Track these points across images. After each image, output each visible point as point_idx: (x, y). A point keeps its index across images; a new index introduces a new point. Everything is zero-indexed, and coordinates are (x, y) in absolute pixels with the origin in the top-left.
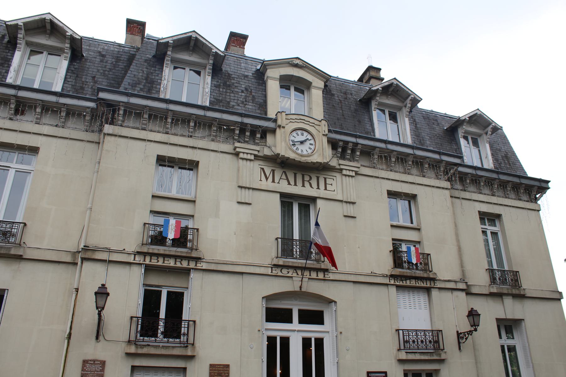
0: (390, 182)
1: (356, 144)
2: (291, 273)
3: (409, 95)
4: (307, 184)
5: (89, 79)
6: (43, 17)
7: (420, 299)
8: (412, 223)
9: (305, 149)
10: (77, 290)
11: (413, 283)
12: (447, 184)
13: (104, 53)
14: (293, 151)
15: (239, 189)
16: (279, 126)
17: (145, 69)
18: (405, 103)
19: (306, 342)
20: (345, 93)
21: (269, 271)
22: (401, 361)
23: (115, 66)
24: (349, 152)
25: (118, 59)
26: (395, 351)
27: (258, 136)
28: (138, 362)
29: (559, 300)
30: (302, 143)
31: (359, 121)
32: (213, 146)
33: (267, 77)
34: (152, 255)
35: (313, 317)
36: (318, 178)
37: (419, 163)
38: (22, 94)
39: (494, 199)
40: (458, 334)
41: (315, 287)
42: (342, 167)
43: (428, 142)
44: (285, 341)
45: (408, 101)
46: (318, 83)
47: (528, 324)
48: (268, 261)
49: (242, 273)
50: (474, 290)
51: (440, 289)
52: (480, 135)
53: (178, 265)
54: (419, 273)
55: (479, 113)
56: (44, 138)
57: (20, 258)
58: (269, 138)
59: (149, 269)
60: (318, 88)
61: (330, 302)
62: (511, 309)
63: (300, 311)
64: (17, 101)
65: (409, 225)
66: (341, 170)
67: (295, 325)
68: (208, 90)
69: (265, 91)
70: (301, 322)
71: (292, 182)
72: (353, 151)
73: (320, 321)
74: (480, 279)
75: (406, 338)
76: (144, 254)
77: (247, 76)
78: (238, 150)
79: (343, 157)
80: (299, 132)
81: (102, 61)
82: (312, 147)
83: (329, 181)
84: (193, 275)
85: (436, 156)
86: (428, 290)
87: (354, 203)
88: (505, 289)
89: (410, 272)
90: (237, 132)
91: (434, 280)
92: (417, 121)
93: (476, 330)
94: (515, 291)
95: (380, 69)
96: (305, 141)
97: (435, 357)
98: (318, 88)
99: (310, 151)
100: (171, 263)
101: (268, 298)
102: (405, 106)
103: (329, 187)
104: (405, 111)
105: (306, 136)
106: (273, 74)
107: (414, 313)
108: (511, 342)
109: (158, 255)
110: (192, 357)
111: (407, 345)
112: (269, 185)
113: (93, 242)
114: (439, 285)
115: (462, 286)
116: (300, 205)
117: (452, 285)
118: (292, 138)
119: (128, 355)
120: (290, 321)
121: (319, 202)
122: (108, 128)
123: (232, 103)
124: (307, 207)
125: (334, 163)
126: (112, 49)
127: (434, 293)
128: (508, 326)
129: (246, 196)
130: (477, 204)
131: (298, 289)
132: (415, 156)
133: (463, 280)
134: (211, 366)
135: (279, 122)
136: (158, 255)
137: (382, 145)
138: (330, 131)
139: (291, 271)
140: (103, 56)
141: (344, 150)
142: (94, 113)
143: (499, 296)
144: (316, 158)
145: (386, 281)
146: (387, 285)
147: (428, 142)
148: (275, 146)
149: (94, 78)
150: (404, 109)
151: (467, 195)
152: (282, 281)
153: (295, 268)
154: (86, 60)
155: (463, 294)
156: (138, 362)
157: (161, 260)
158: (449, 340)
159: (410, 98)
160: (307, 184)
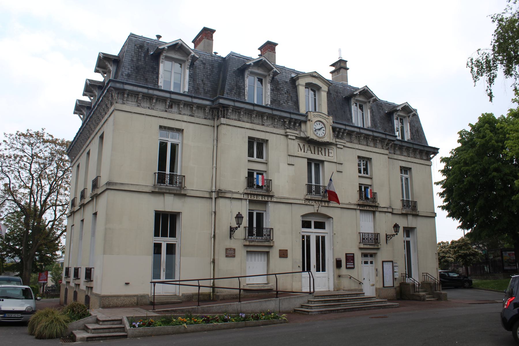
0: (359, 151)
1: (345, 130)
2: (313, 203)
3: (372, 96)
4: (320, 153)
5: (201, 83)
6: (177, 42)
7: (370, 217)
8: (367, 174)
9: (321, 133)
10: (215, 213)
11: (368, 208)
12: (386, 152)
13: (204, 62)
14: (316, 135)
15: (289, 157)
16: (309, 120)
17: (234, 79)
18: (369, 100)
19: (318, 238)
20: (337, 92)
21: (303, 202)
22: (361, 249)
23: (212, 71)
24: (341, 134)
25: (212, 66)
26: (358, 244)
27: (298, 125)
28: (249, 249)
29: (434, 217)
30: (319, 129)
31: (344, 112)
32: (275, 130)
33: (299, 84)
34: (251, 194)
35: (320, 225)
36: (325, 149)
37: (375, 139)
38: (174, 96)
39: (409, 159)
40: (387, 235)
41: (324, 211)
42: (337, 143)
43: (379, 125)
44: (308, 237)
45: (372, 100)
46: (325, 88)
47: (419, 232)
48: (302, 197)
49: (291, 203)
50: (395, 212)
51: (380, 211)
52: (405, 117)
53: (263, 199)
54: (371, 204)
55: (407, 105)
56: (185, 123)
57: (185, 195)
58: (303, 126)
59: (251, 201)
60: (325, 91)
61: (329, 217)
62: (411, 222)
63: (315, 222)
64: (170, 101)
65: (365, 175)
66: (337, 144)
67: (313, 230)
68: (269, 93)
69: (297, 93)
70: (315, 228)
71: (313, 152)
72: (343, 133)
73: (324, 228)
74: (398, 206)
75: (364, 237)
76: (248, 194)
77: (286, 82)
78: (288, 134)
79: (337, 137)
80: (318, 123)
81: (204, 68)
82: (324, 132)
83: (330, 151)
84: (270, 204)
85: (384, 136)
86: (374, 212)
87: (342, 164)
88: (409, 211)
89: (367, 202)
90: (287, 123)
91: (377, 207)
92: (374, 110)
93: (397, 234)
94: (414, 213)
95: (345, 62)
96: (321, 128)
97: (376, 247)
98: (325, 91)
99: (323, 135)
100: (260, 198)
101: (303, 216)
102: (369, 102)
103: (330, 155)
104: (368, 105)
105: (321, 125)
106: (302, 82)
107: (366, 224)
108: (408, 239)
109: (254, 194)
111: (364, 241)
112: (301, 153)
113: (223, 187)
114: (380, 209)
115: (390, 210)
116: (315, 165)
117: (385, 210)
118: (315, 127)
119: (245, 246)
120: (311, 228)
121: (326, 163)
122: (223, 120)
123: (281, 102)
124: (319, 165)
125: (334, 142)
126: (208, 58)
127: (377, 214)
128: (408, 231)
129: (292, 160)
130: (400, 162)
131: (316, 211)
132: (373, 136)
133: (390, 207)
134: (280, 250)
135: (309, 118)
136: (254, 194)
137: (358, 130)
138: (333, 122)
139: (313, 202)
140: (204, 64)
141: (339, 132)
142: (212, 109)
143: (405, 215)
144: (326, 139)
145: (355, 207)
146: (356, 209)
147: (379, 125)
148: (306, 132)
149: (202, 80)
150: (368, 103)
151: (395, 157)
152: (309, 207)
153: (315, 200)
154: (196, 67)
155: (390, 215)
156: (249, 249)
157: (255, 197)
158: (382, 238)
159: (373, 98)
160: (320, 153)
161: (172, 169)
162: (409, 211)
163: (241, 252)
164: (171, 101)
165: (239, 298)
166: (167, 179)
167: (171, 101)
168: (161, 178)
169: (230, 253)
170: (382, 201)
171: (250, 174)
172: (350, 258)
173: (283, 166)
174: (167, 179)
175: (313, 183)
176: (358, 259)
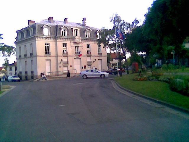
38: (47, 37)
46: (79, 30)
57: (51, 56)
62: (100, 58)
86: (90, 57)
107: (89, 59)
110: (68, 65)
112: (74, 45)
122: (57, 41)
143: (99, 56)
161: (48, 51)
162: (100, 55)
163: (62, 66)
164: (46, 38)
165: (63, 75)
166: (47, 53)
167: (46, 38)
168: (46, 53)
169: (60, 67)
170: (92, 54)
171: (63, 51)
172: (85, 67)
173: (70, 48)
174: (47, 53)
175: (77, 51)
176: (87, 66)
